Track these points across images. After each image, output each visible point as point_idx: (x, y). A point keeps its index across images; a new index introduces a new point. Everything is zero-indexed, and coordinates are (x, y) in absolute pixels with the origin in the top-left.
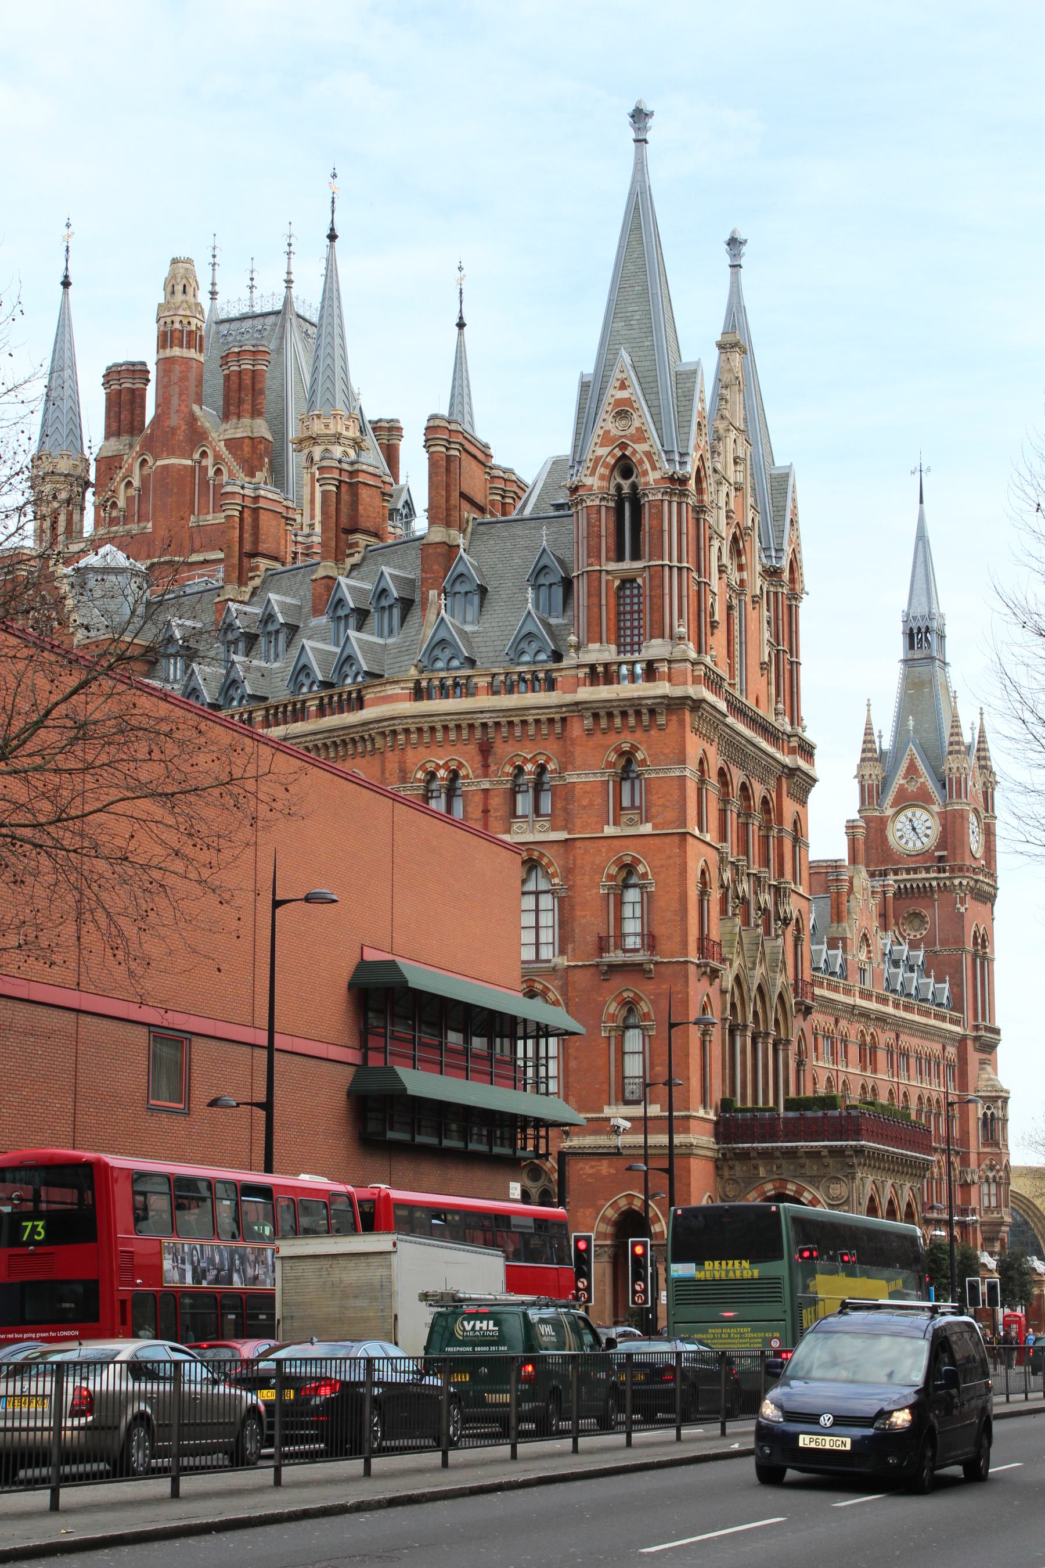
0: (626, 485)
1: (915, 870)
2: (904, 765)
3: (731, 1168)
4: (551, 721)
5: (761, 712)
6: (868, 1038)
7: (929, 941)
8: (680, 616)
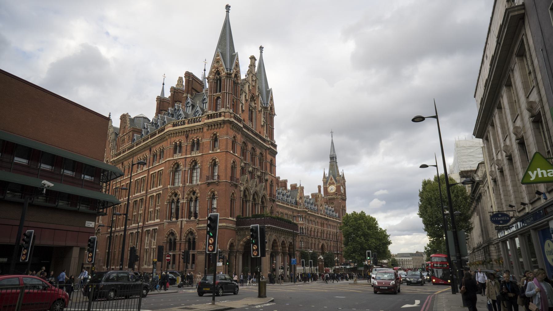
0: (218, 77)
1: (332, 195)
2: (330, 178)
3: (240, 232)
4: (200, 129)
5: (257, 132)
6: (322, 222)
7: (335, 207)
8: (229, 103)
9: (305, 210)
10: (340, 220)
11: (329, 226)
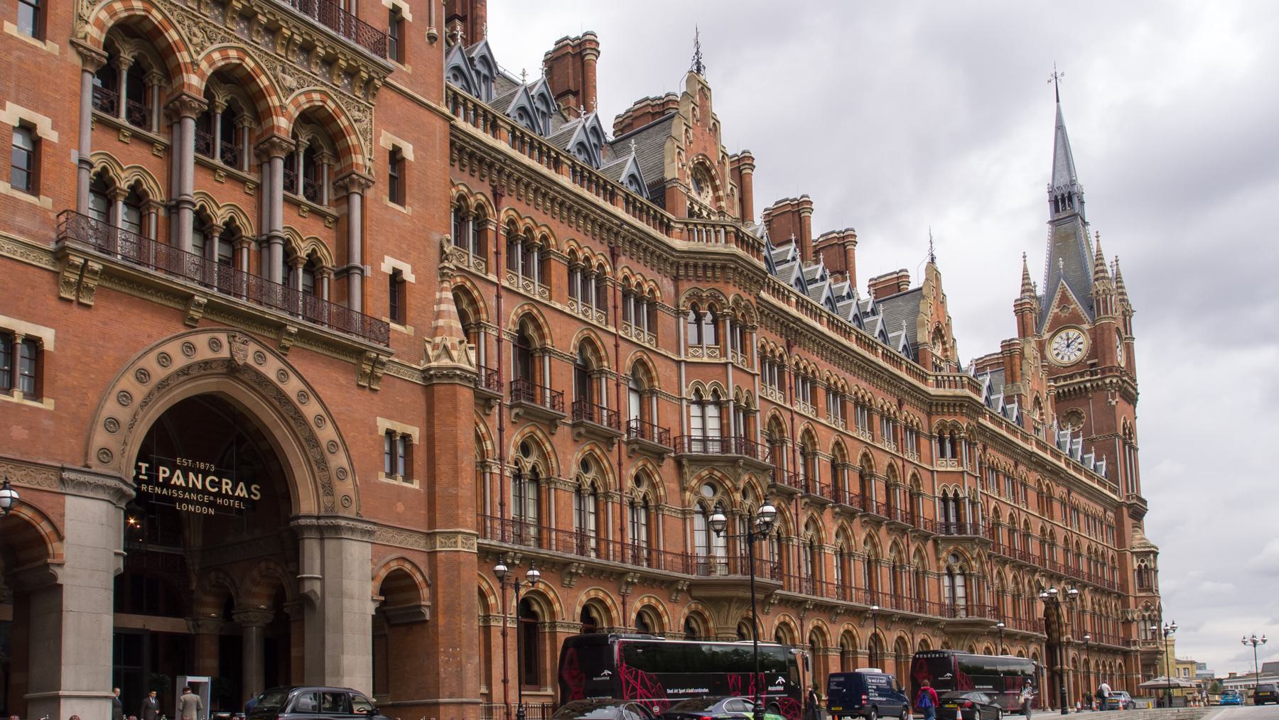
9: (967, 392)
10: (1114, 491)
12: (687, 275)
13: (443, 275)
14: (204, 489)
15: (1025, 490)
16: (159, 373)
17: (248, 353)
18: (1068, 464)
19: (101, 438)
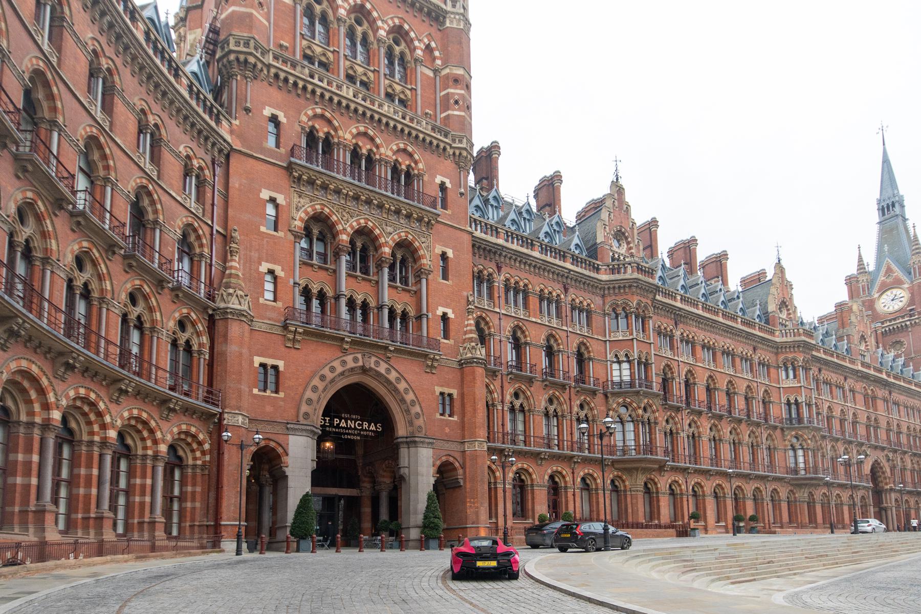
11: (895, 408)
12: (609, 293)
13: (468, 312)
14: (355, 428)
15: (854, 394)
16: (330, 376)
17: (371, 362)
18: (889, 376)
19: (304, 408)
